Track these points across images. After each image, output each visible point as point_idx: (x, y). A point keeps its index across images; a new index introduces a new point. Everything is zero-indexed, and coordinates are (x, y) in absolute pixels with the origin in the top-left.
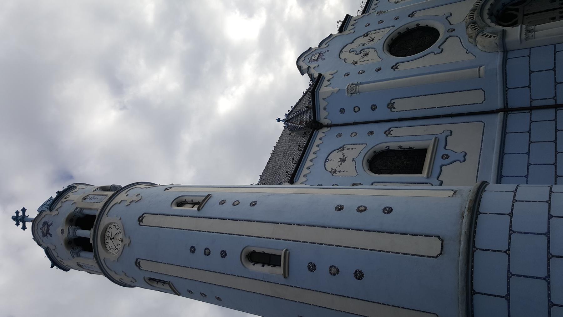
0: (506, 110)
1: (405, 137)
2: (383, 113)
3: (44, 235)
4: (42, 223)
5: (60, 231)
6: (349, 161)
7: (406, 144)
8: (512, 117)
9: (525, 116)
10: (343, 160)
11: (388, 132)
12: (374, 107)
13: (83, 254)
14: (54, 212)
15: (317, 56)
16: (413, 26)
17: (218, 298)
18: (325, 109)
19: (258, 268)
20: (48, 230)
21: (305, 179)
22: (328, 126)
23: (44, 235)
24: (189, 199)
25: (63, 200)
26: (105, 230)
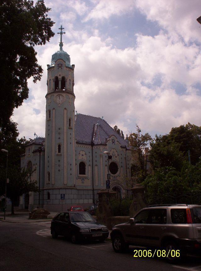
0: (93, 190)
1: (88, 169)
2: (95, 163)
3: (58, 65)
4: (62, 63)
5: (60, 74)
6: (83, 157)
7: (86, 170)
8: (92, 191)
9: (92, 193)
10: (83, 155)
11: (89, 165)
12: (96, 161)
13: (54, 83)
14: (65, 68)
15: (114, 141)
16: (118, 167)
17: (49, 135)
18: (97, 148)
19: (57, 148)
20: (60, 67)
21: (77, 146)
22: (92, 148)
23: (58, 65)
24: (71, 122)
25: (69, 70)
26: (62, 95)
